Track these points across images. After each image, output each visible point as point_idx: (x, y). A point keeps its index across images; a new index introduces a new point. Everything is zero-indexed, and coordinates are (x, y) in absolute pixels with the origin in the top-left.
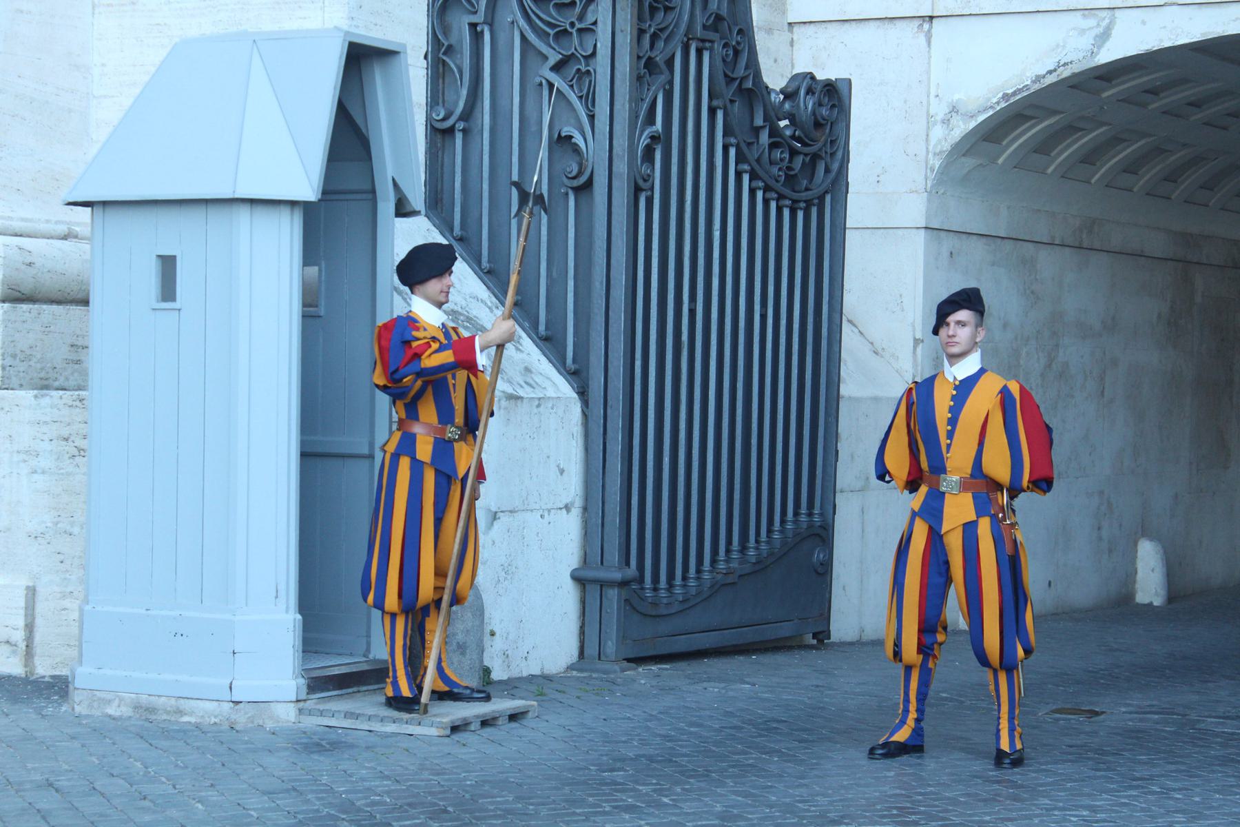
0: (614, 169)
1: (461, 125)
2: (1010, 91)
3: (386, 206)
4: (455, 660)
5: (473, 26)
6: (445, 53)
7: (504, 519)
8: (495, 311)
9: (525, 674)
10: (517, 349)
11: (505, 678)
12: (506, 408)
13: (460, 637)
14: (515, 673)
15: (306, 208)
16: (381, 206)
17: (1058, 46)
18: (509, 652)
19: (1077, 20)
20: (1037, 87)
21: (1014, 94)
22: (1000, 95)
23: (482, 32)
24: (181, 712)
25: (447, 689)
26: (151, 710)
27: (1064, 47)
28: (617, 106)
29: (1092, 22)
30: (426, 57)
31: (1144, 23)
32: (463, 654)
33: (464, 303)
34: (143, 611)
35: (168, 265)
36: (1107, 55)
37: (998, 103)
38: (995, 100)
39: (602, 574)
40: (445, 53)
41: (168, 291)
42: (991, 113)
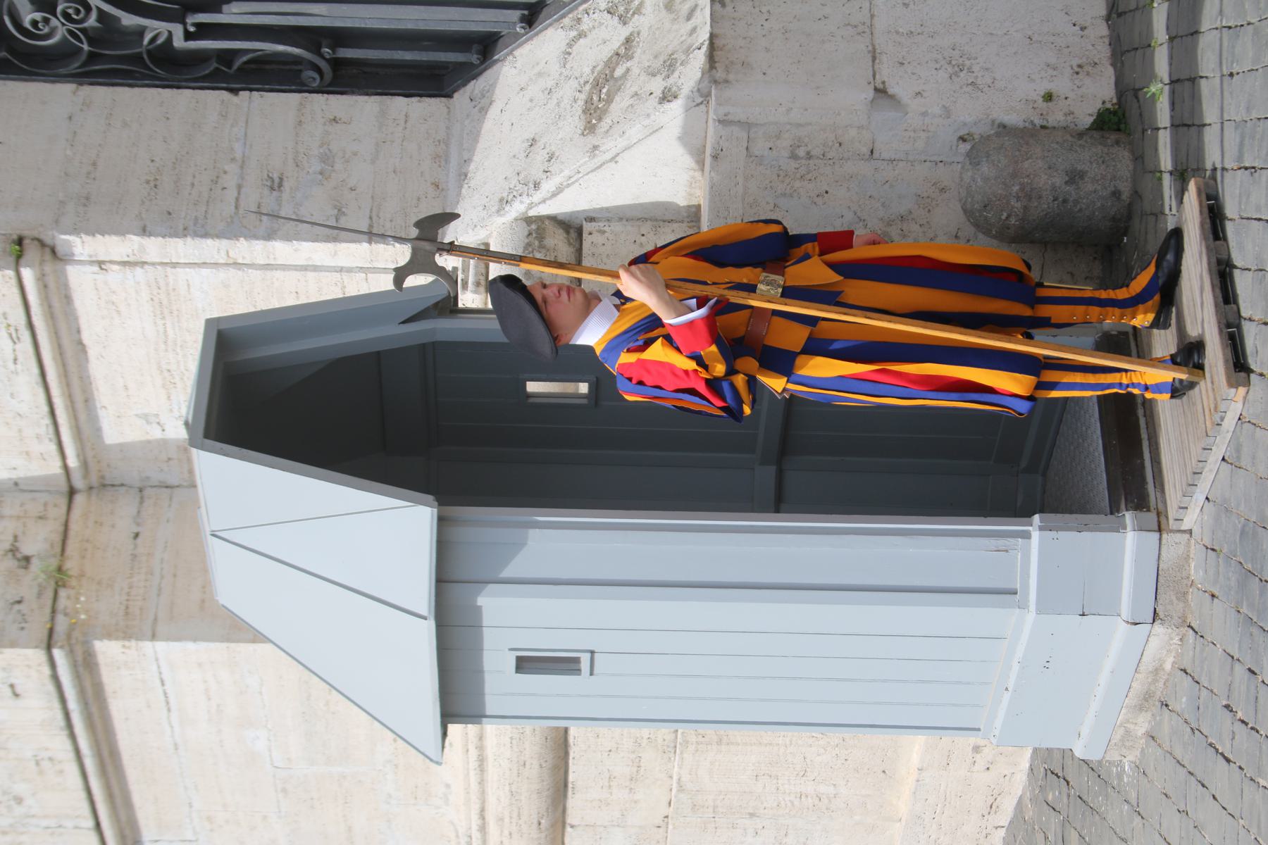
1: (326, 50)
3: (443, 328)
4: (1090, 187)
5: (188, 36)
6: (230, 68)
7: (886, 73)
8: (584, 27)
9: (1103, 30)
10: (638, 11)
11: (1110, 71)
12: (727, 71)
13: (1059, 180)
14: (1102, 51)
16: (440, 337)
18: (1075, 62)
23: (199, 26)
24: (1157, 671)
25: (1157, 297)
26: (1147, 696)
30: (234, 91)
32: (1082, 175)
33: (574, 84)
34: (1007, 696)
35: (525, 664)
40: (230, 68)
41: (565, 665)
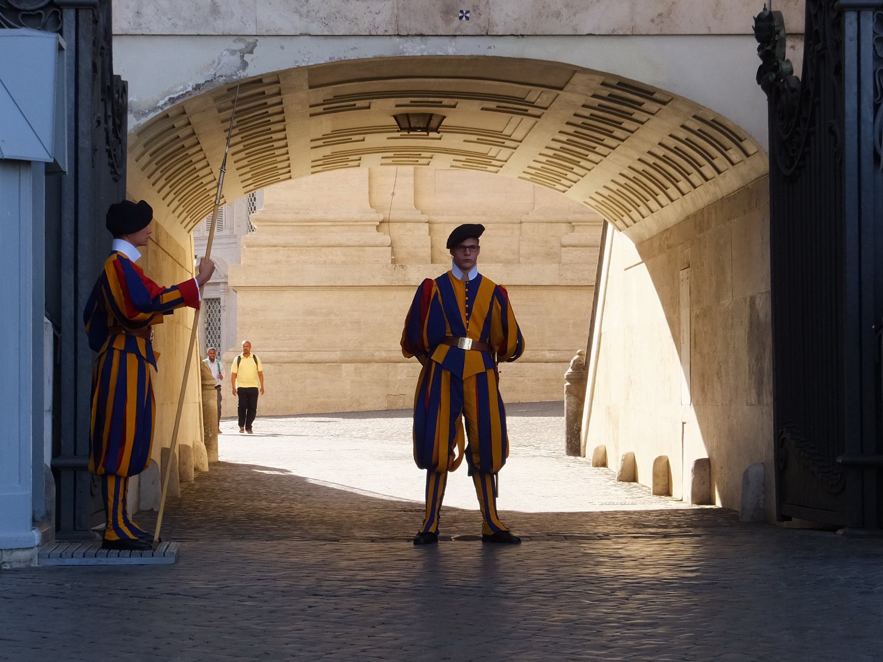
0: (80, 145)
2: (176, 96)
15: (47, 164)
17: (214, 62)
19: (230, 43)
20: (198, 93)
21: (179, 97)
22: (167, 99)
27: (219, 63)
28: (82, 96)
29: (241, 46)
31: (282, 48)
36: (252, 72)
37: (165, 104)
38: (161, 103)
39: (78, 461)
42: (160, 111)
